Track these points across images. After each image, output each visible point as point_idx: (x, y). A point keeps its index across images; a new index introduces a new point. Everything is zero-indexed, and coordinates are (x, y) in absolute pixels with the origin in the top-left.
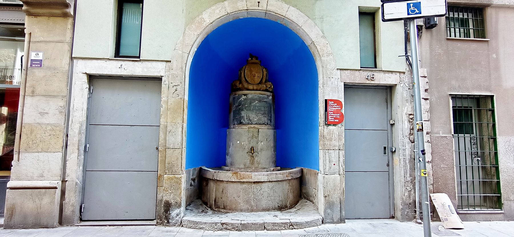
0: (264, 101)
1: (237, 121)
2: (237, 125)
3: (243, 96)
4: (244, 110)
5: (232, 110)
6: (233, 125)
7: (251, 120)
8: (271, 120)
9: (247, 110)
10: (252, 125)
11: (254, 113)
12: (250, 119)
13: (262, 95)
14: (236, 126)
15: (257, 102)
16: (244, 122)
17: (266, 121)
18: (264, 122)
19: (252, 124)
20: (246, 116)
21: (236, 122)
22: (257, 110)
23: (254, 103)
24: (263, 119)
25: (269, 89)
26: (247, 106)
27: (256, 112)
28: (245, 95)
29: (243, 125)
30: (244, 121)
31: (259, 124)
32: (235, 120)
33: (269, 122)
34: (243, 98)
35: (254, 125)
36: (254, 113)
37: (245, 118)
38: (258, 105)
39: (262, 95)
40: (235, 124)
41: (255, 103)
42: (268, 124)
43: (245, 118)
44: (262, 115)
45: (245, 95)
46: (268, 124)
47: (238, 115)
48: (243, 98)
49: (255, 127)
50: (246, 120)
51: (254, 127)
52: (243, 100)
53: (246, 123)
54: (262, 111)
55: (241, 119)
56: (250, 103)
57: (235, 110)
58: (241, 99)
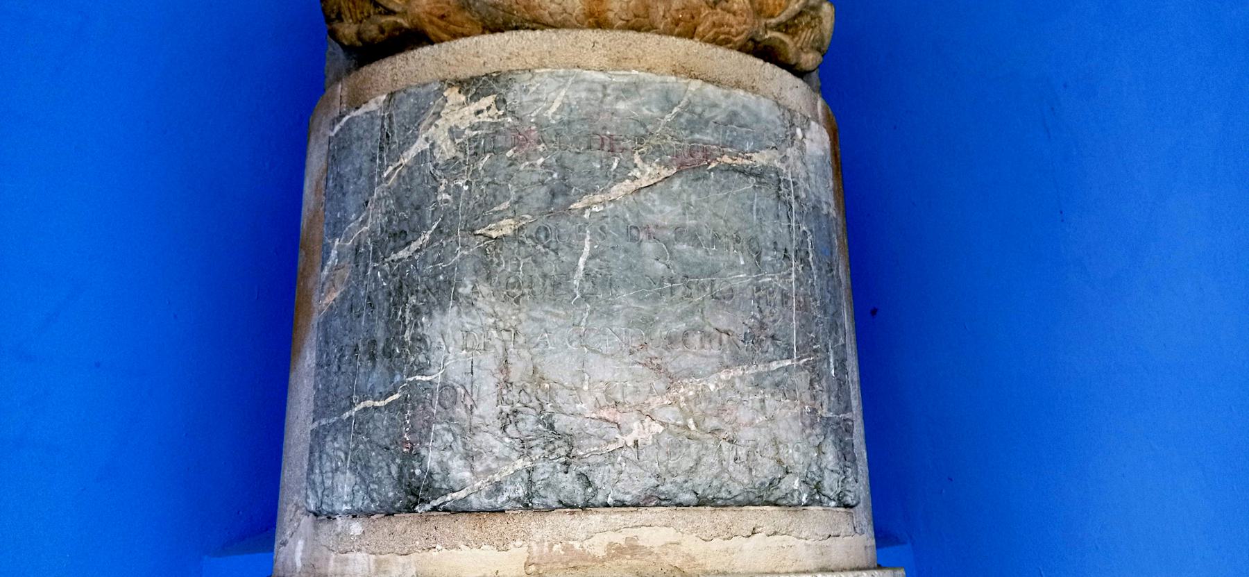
0: (745, 172)
1: (362, 467)
2: (356, 528)
3: (453, 95)
4: (465, 290)
5: (316, 318)
6: (307, 521)
7: (570, 440)
8: (849, 431)
9: (513, 293)
10: (595, 519)
11: (619, 324)
12: (561, 422)
13: (717, 83)
14: (345, 546)
15: (647, 173)
16: (459, 470)
17: (794, 456)
18: (766, 469)
19: (586, 506)
20: (488, 386)
21: (345, 484)
22: (659, 288)
23: (618, 190)
24: (744, 415)
25: (786, 39)
26: (507, 227)
27: (647, 323)
28: (473, 86)
29: (445, 524)
30: (469, 457)
31: (702, 502)
32: (336, 446)
33: (830, 458)
34: (454, 133)
35: (617, 517)
36: (619, 324)
37: (487, 409)
38: (665, 213)
39: (710, 88)
40: (331, 517)
41: (628, 186)
42: (816, 494)
43: (487, 409)
44: (738, 360)
45: (473, 86)
46: (818, 488)
47: (377, 376)
48: (454, 133)
49: (633, 548)
50: (491, 441)
51: (617, 552)
52: (446, 150)
53: (498, 488)
54: (722, 299)
55: (423, 434)
56: (560, 192)
57: (349, 306)
58: (420, 145)
